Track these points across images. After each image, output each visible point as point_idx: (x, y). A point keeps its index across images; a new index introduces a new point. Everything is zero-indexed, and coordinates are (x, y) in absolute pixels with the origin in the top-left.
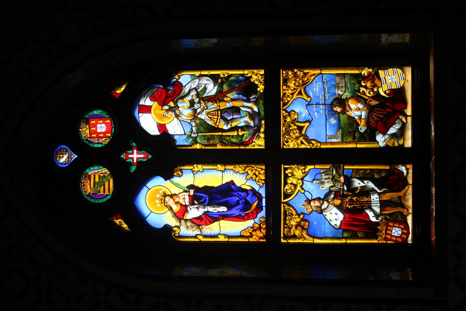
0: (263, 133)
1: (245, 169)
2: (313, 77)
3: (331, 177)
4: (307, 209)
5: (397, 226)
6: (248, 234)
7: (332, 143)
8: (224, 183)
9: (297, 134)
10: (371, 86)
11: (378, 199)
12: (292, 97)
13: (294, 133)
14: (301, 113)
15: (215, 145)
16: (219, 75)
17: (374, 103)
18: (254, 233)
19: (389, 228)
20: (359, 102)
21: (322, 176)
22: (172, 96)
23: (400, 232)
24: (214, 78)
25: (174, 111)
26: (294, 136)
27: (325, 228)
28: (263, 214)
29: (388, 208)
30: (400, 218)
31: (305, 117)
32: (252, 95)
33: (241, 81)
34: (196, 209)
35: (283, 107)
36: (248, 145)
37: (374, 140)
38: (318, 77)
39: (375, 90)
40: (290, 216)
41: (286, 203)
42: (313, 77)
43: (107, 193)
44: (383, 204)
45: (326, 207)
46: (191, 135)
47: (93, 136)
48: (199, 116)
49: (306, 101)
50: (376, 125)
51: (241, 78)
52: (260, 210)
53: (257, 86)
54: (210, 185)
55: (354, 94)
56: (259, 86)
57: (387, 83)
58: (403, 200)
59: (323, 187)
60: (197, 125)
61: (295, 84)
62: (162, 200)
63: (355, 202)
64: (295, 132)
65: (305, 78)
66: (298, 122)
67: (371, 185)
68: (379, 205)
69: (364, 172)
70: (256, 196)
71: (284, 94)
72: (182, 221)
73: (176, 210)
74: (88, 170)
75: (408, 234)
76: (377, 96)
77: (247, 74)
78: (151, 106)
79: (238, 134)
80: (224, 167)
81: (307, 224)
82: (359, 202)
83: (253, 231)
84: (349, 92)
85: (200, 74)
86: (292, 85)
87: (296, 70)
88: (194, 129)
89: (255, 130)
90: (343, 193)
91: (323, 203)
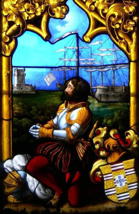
2: (125, 48)
7: (10, 77)
10: (108, 146)
12: (91, 10)
13: (28, 10)
17: (81, 150)
26: (23, 10)
31: (57, 32)
38: (124, 56)
42: (125, 48)
49: (85, 35)
50: (42, 154)
57: (114, 173)
61: (113, 16)
64: (31, 12)
76: (92, 155)
84: (99, 108)
87: (135, 18)
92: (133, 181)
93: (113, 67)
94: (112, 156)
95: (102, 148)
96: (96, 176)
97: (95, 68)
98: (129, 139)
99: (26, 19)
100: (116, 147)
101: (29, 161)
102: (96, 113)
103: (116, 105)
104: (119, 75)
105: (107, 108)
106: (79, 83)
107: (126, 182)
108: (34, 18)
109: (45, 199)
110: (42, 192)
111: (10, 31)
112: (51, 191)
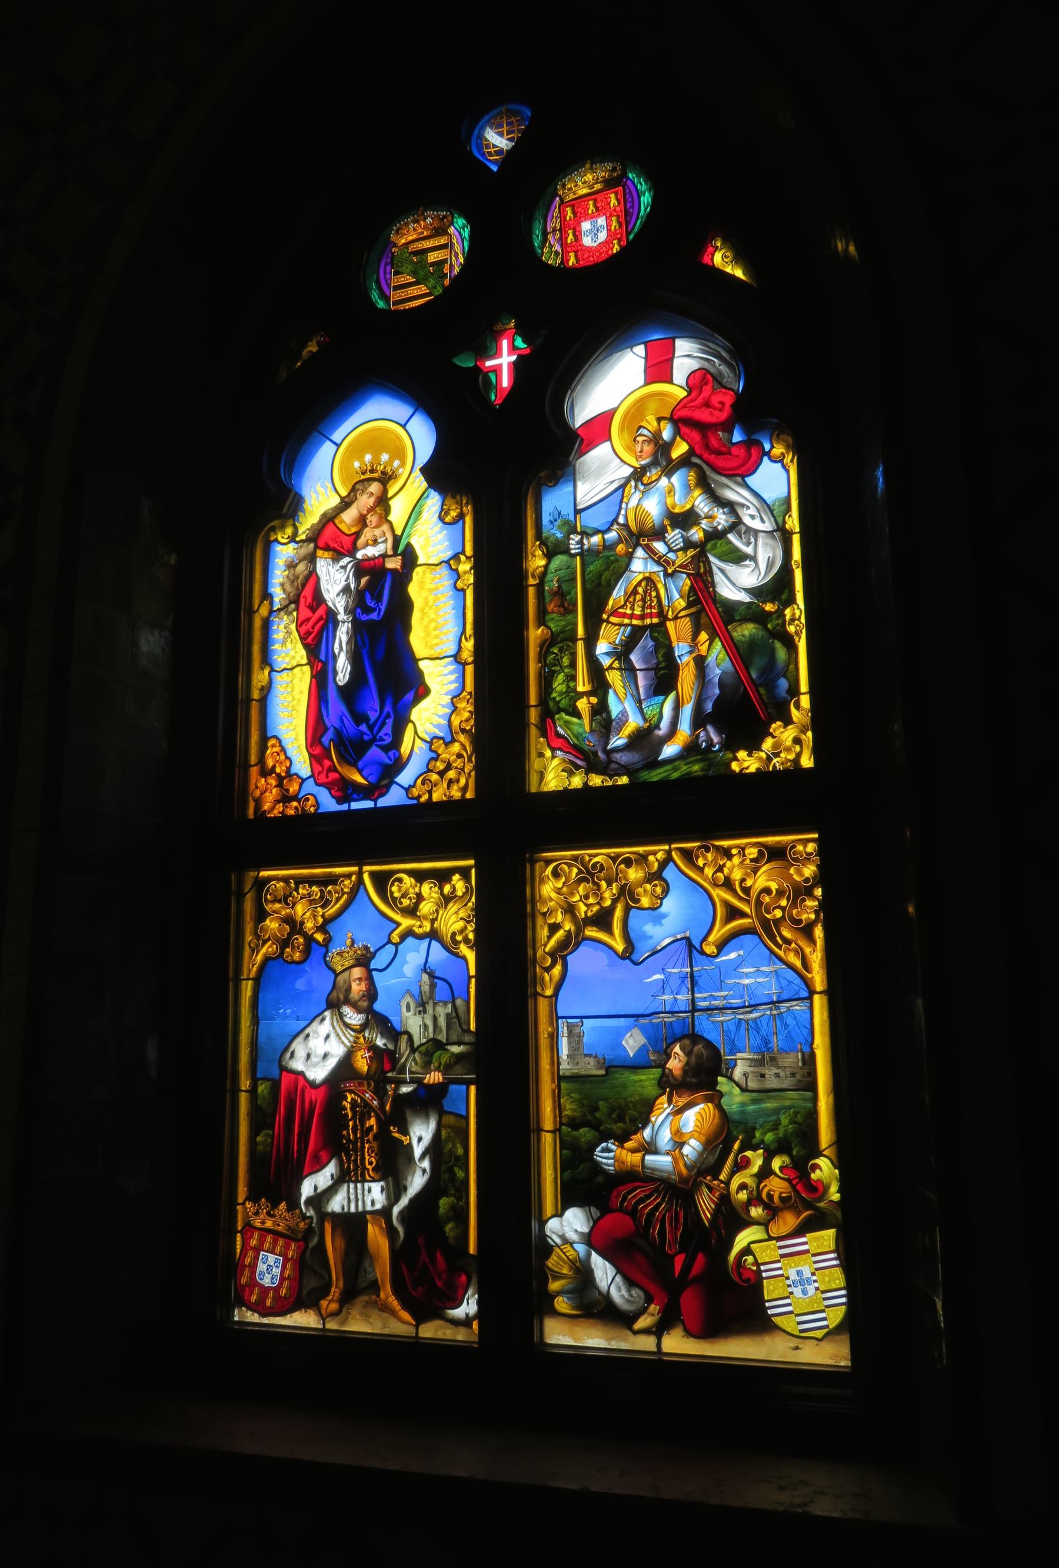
0: (586, 784)
1: (463, 731)
2: (798, 963)
3: (442, 1037)
4: (340, 954)
5: (287, 1273)
6: (270, 763)
7: (554, 1038)
8: (422, 665)
9: (583, 908)
11: (369, 1208)
12: (715, 885)
13: (587, 897)
14: (658, 920)
15: (541, 621)
16: (791, 601)
17: (706, 1204)
19: (281, 1242)
20: (709, 1144)
21: (445, 1003)
22: (707, 447)
23: (267, 1281)
24: (778, 588)
25: (655, 463)
26: (577, 898)
27: (286, 1017)
28: (329, 803)
29: (340, 1243)
30: (311, 1283)
31: (646, 937)
32: (719, 732)
33: (770, 685)
34: (343, 583)
35: (680, 849)
36: (544, 733)
37: (571, 1196)
38: (798, 981)
39: (756, 1212)
40: (322, 897)
41: (360, 882)
42: (798, 963)
43: (395, 296)
44: (352, 1225)
45: (347, 1020)
46: (575, 532)
47: (569, 210)
48: (640, 553)
51: (783, 684)
52: (337, 794)
53: (753, 746)
54: (416, 618)
55: (738, 1123)
56: (756, 754)
57: (785, 1261)
58: (366, 1298)
59: (408, 1009)
60: (608, 547)
61: (767, 891)
62: (372, 471)
63: (362, 1124)
64: (591, 901)
65: (791, 929)
66: (627, 910)
67: (417, 1182)
68: (353, 1209)
69: (457, 1159)
70: (381, 778)
71: (727, 853)
72: (312, 545)
73: (342, 521)
74: (460, 222)
76: (732, 1218)
77: (798, 706)
78: (669, 380)
79: (582, 695)
80: (470, 659)
81: (297, 956)
82: (362, 1138)
83: (278, 775)
84: (743, 1104)
85: (791, 533)
86: (764, 879)
87: (818, 892)
88: (596, 539)
89: (595, 754)
90: (391, 1081)
91: (359, 1012)
92: (834, 1286)
93: (771, 1010)
94: (780, 1220)
95: (755, 1199)
96: (745, 1268)
97: (729, 1011)
98: (819, 1181)
99: (583, 915)
100: (789, 1198)
101: (595, 1222)
102: (737, 1117)
103: (784, 1098)
104: (787, 1026)
105: (763, 1106)
106: (696, 1049)
107: (816, 1285)
108: (598, 912)
109: (631, 1312)
110: (622, 1296)
111: (552, 943)
112: (641, 1294)
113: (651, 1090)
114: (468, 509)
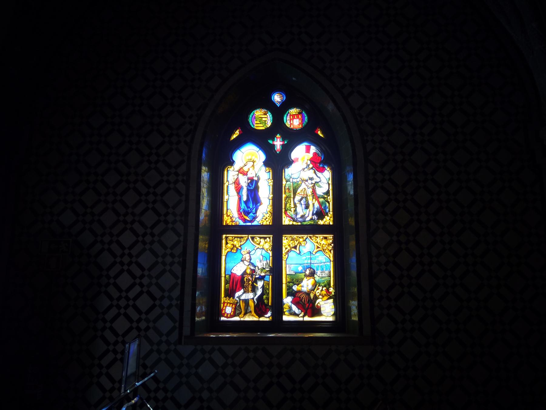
6: (229, 214)
7: (286, 267)
15: (285, 194)
16: (329, 196)
17: (312, 296)
18: (229, 218)
20: (313, 286)
23: (228, 312)
28: (242, 223)
29: (244, 304)
30: (237, 312)
33: (326, 210)
37: (288, 295)
43: (256, 125)
44: (246, 302)
51: (328, 210)
53: (322, 219)
67: (259, 292)
71: (317, 237)
74: (270, 113)
75: (227, 317)
76: (316, 298)
95: (320, 295)
113: (303, 277)
114: (271, 171)
